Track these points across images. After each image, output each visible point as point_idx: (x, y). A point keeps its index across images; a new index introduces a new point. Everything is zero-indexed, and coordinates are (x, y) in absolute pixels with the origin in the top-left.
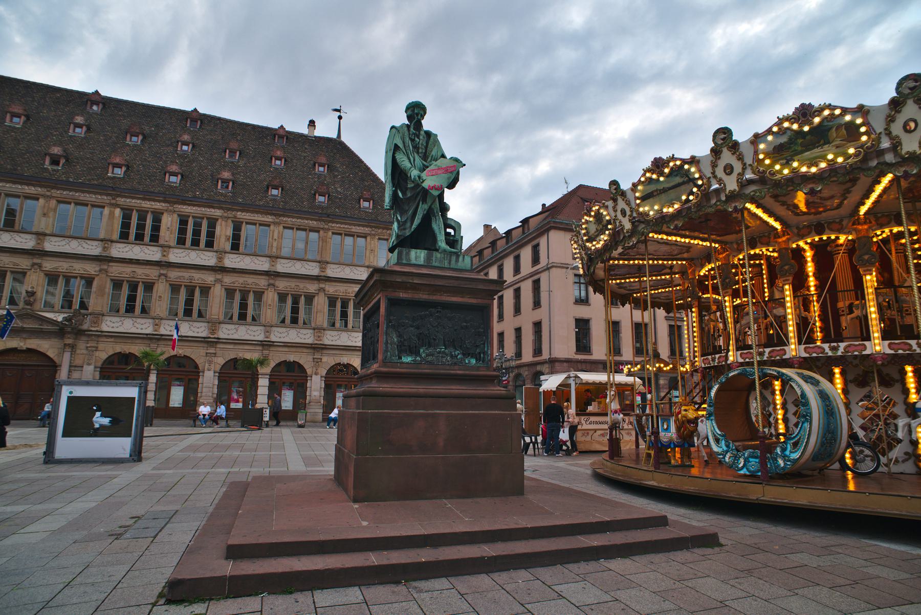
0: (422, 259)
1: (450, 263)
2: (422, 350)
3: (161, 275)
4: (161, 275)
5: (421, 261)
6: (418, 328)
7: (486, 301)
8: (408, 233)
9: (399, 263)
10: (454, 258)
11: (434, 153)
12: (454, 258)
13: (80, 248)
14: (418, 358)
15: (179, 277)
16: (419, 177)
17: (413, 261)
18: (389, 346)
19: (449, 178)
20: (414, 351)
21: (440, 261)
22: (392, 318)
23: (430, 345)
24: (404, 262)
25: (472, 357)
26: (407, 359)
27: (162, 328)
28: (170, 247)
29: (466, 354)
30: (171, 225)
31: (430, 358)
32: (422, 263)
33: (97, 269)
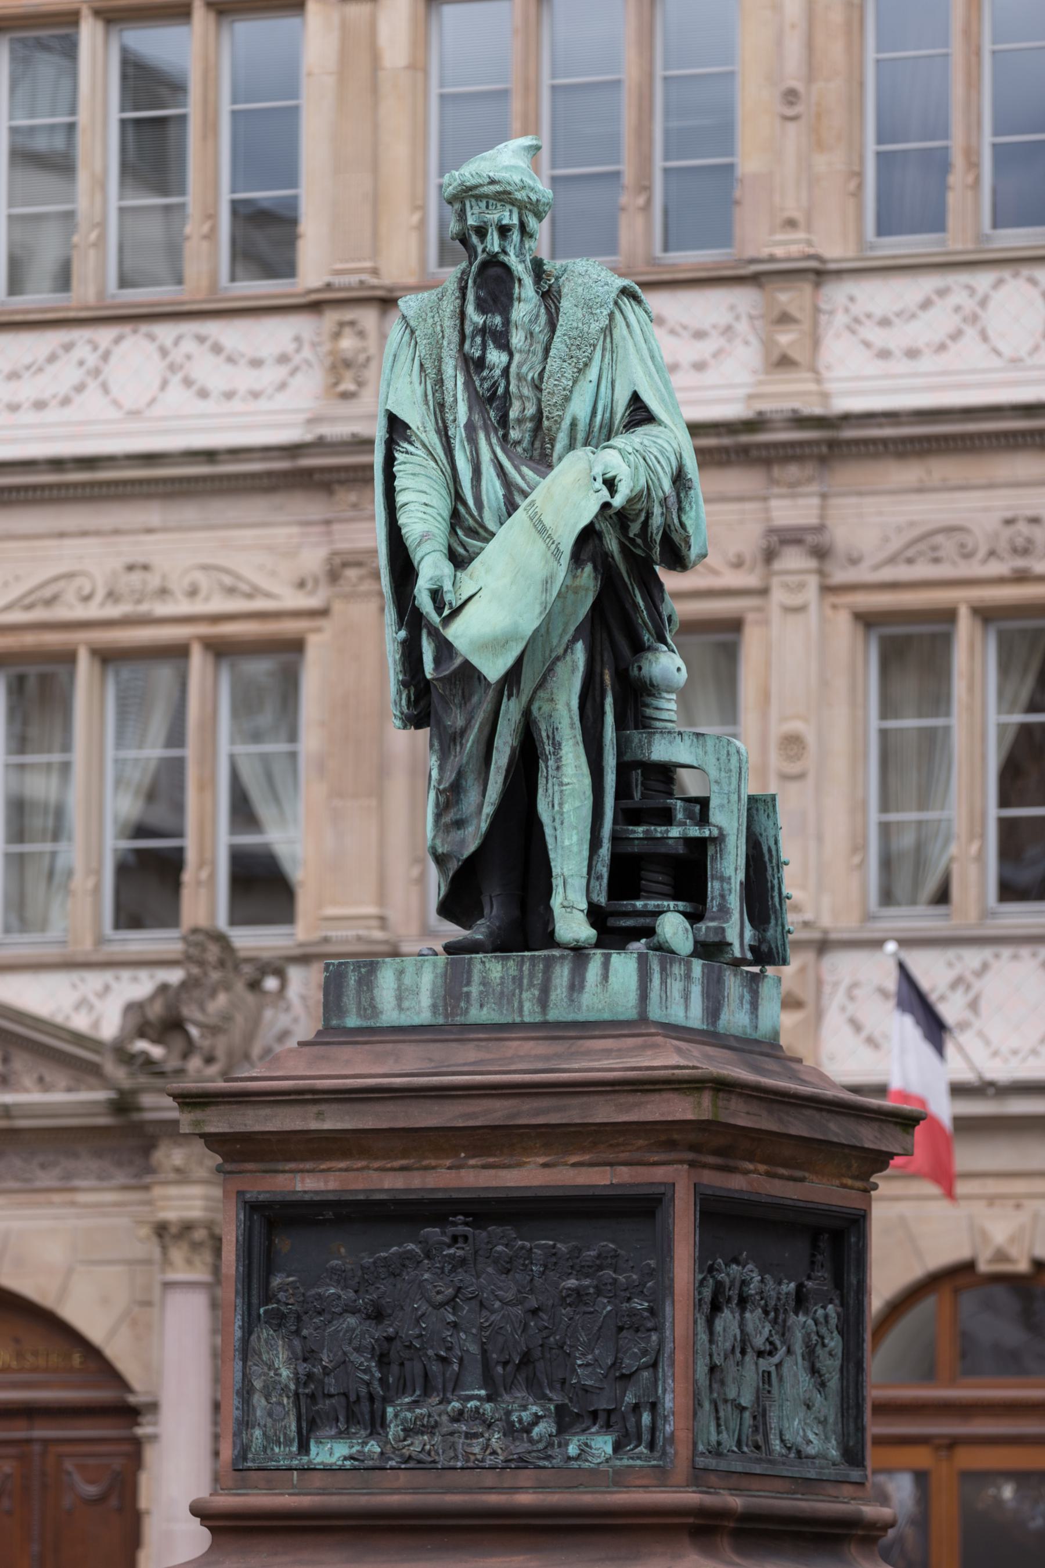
0: (425, 1000)
1: (543, 1002)
2: (390, 1410)
3: (779, 541)
4: (779, 541)
6: (377, 1315)
7: (660, 1174)
8: (471, 839)
9: (332, 1033)
10: (562, 974)
11: (579, 407)
12: (562, 974)
13: (177, 397)
14: (374, 1447)
15: (926, 542)
16: (436, 595)
17: (390, 1015)
18: (259, 1401)
19: (547, 582)
20: (363, 1414)
21: (504, 998)
22: (276, 1281)
23: (427, 1389)
24: (352, 1021)
25: (608, 1426)
26: (330, 1452)
27: (834, 1021)
28: (819, 274)
29: (566, 1421)
30: (811, 73)
31: (416, 1445)
32: (425, 1017)
33: (313, 558)
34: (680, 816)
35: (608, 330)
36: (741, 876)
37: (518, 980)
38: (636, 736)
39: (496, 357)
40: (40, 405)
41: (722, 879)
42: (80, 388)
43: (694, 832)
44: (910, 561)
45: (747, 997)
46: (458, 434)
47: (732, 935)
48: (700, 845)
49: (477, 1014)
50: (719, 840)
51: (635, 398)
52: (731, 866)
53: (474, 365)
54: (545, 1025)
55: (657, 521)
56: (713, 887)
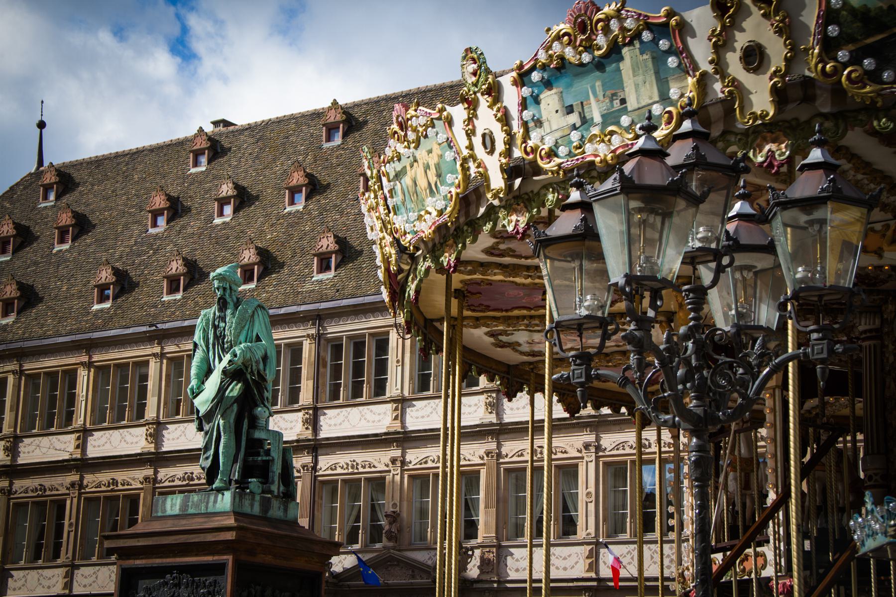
0: (178, 507)
5: (176, 511)
17: (169, 512)
24: (160, 514)
34: (262, 454)
35: (253, 316)
36: (279, 471)
37: (201, 500)
38: (251, 431)
39: (222, 325)
40: (423, 417)
41: (274, 472)
42: (431, 413)
43: (264, 458)
44: (618, 449)
45: (282, 507)
46: (211, 346)
47: (274, 488)
48: (268, 461)
49: (191, 511)
50: (273, 460)
51: (257, 335)
52: (277, 468)
53: (215, 327)
54: (207, 513)
55: (254, 368)
56: (271, 474)
